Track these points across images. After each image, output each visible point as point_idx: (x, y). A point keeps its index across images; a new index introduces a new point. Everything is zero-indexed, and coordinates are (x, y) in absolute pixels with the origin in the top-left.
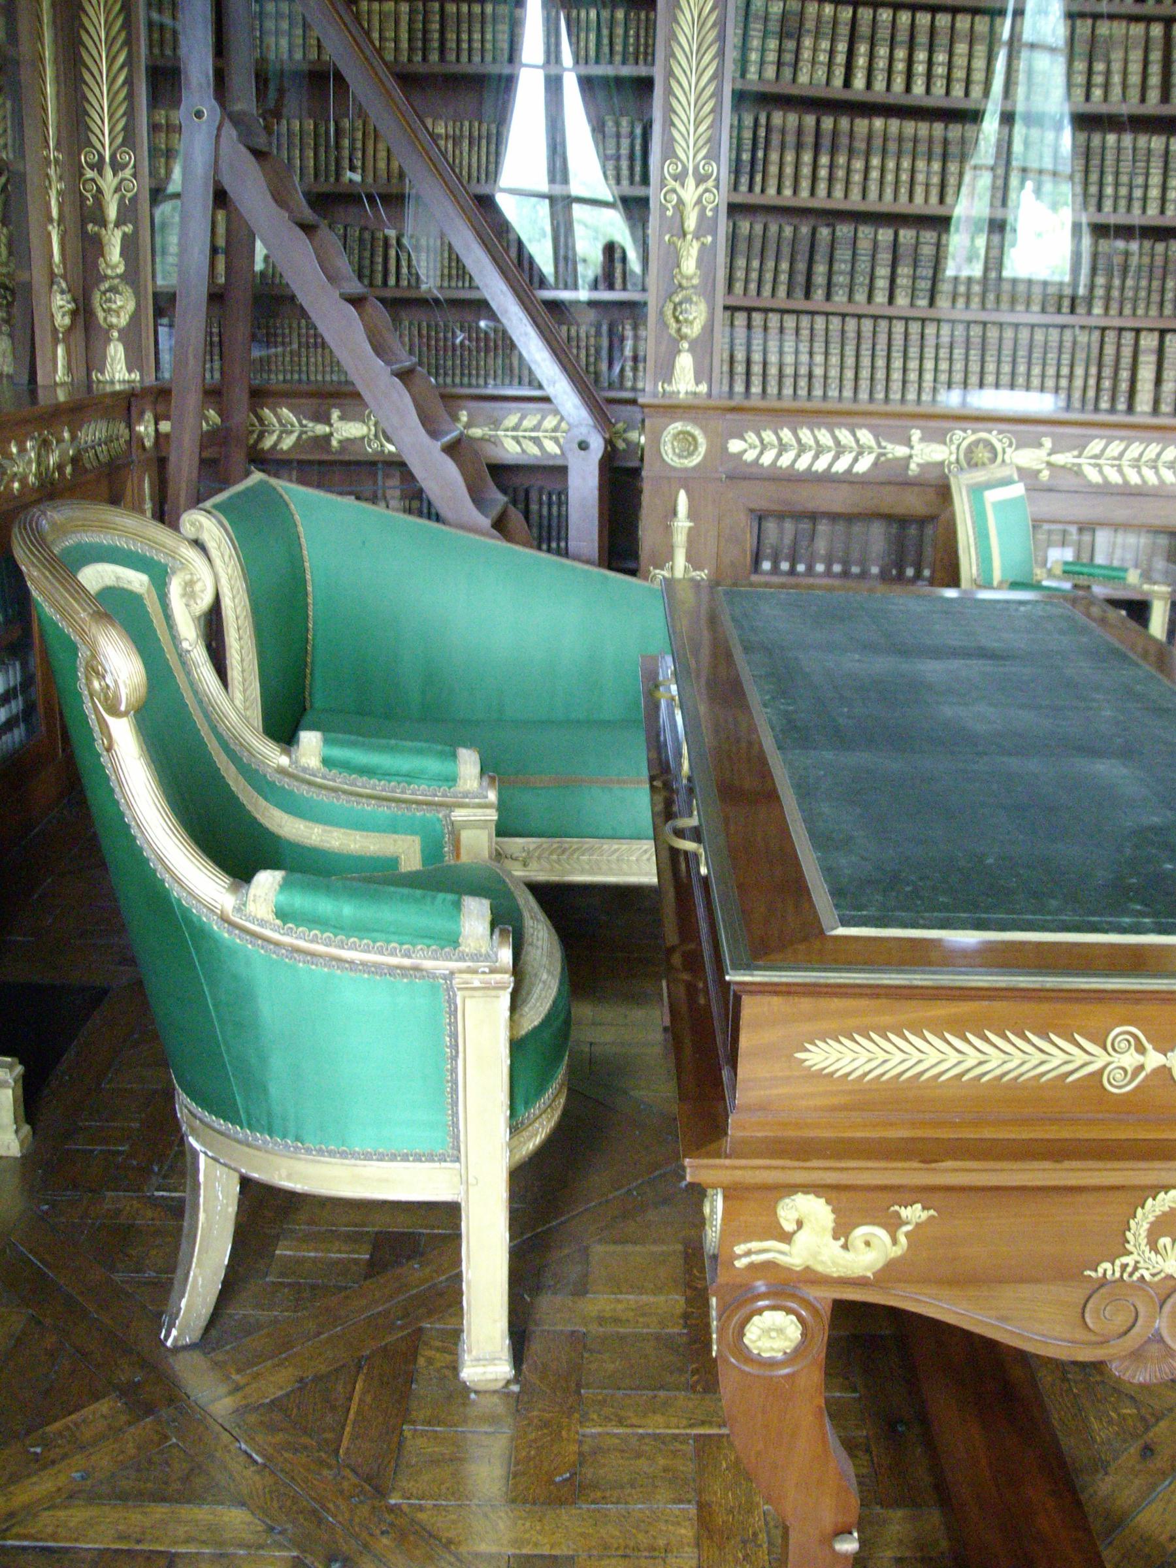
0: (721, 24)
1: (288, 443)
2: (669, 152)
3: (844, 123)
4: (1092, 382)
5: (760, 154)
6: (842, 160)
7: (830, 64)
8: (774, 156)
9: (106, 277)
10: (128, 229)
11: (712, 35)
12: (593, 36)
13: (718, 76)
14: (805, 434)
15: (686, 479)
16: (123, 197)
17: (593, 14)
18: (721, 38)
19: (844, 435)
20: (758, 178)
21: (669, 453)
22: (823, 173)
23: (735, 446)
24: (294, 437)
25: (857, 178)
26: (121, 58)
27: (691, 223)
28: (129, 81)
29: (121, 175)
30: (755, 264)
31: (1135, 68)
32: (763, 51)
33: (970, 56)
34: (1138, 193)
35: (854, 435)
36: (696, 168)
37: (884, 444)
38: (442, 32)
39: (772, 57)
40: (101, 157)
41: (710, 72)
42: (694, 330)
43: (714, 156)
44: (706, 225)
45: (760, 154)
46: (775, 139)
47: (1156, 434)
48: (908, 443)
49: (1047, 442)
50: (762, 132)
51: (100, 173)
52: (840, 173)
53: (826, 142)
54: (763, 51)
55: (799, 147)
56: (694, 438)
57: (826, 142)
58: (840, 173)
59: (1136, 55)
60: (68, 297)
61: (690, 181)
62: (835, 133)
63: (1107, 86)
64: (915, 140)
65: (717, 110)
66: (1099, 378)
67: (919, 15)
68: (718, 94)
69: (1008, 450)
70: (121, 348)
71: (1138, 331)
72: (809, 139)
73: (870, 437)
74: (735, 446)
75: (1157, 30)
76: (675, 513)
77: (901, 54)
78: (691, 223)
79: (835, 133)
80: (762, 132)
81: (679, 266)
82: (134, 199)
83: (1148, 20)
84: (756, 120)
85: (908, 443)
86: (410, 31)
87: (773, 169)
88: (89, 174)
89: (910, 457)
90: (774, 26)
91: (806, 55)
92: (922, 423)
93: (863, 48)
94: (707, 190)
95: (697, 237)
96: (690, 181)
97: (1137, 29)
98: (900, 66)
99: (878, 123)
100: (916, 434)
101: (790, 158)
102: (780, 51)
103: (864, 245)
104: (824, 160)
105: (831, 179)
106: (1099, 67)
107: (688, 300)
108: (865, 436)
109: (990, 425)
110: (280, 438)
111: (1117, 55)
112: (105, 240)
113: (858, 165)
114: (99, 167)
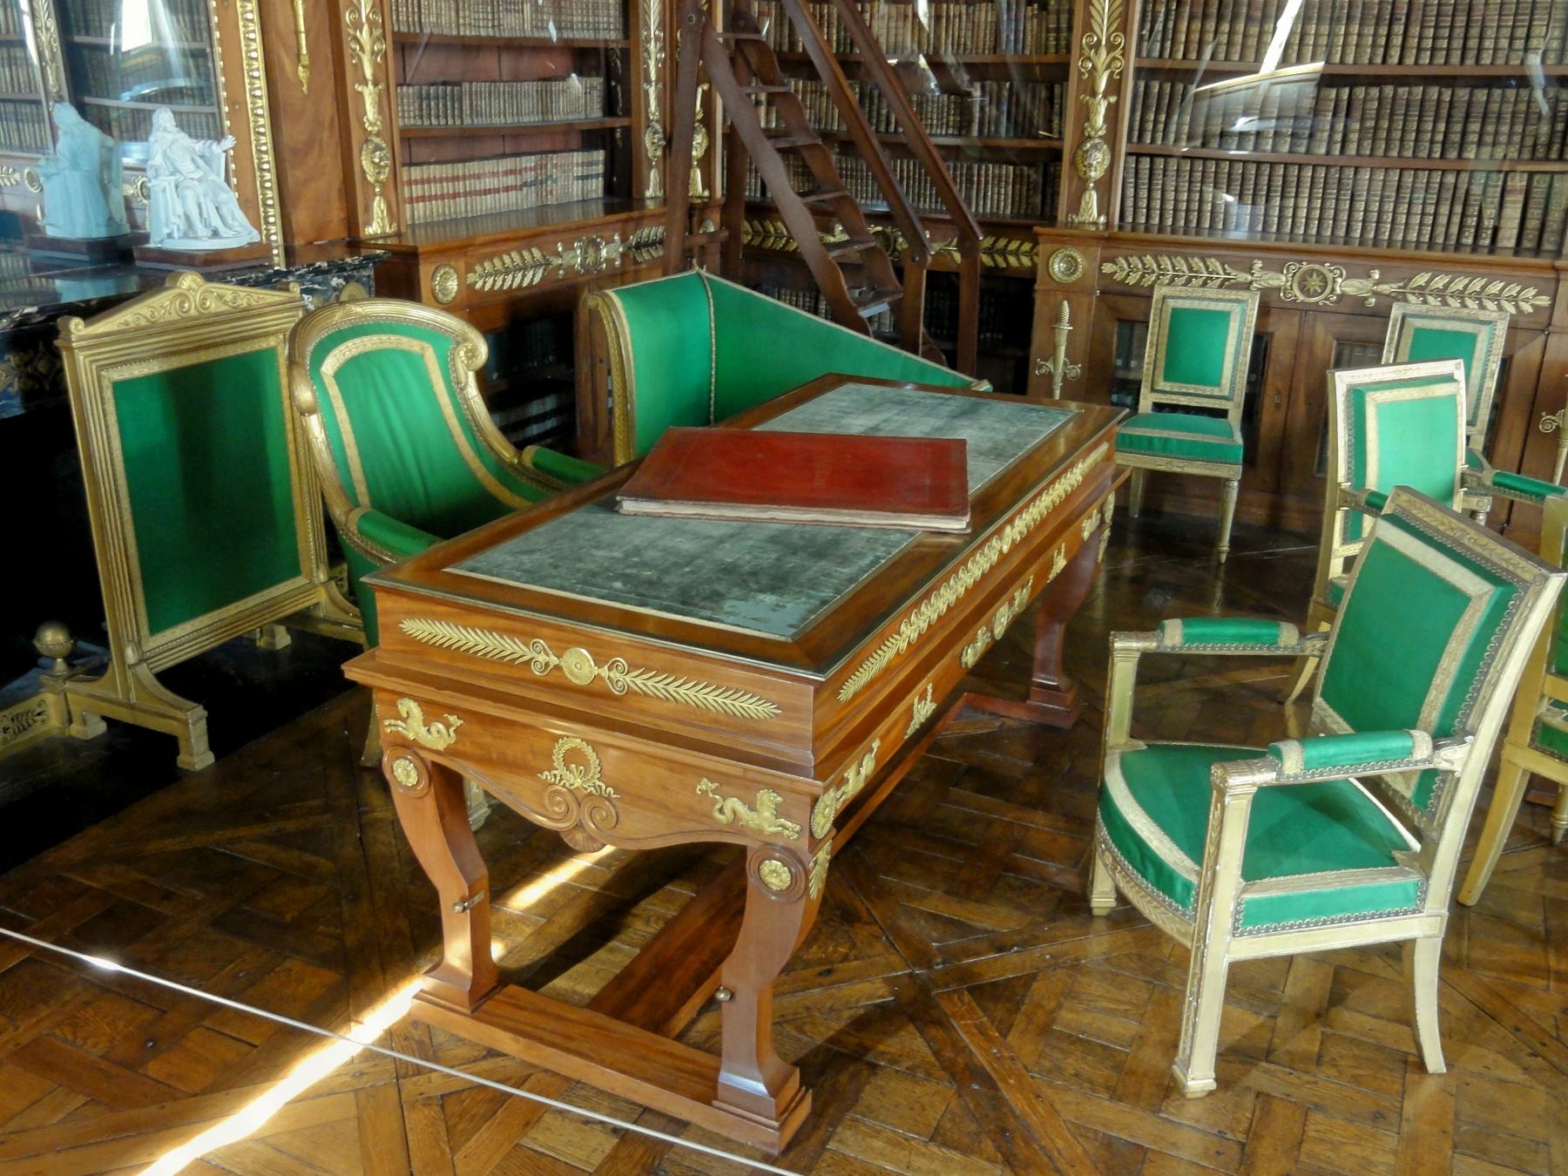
2: (1088, 28)
4: (1456, 219)
5: (1171, 25)
6: (1240, 27)
8: (1184, 26)
15: (1068, 291)
19: (1197, 263)
20: (1168, 44)
21: (1058, 267)
23: (1108, 268)
27: (1102, 85)
30: (1163, 117)
35: (1205, 264)
36: (1108, 39)
37: (1229, 270)
42: (1095, 174)
43: (1124, 28)
45: (1171, 25)
48: (1249, 270)
52: (1239, 39)
56: (1073, 258)
58: (1239, 39)
60: (661, 136)
61: (1103, 52)
66: (1464, 215)
69: (1339, 280)
73: (1218, 264)
74: (1108, 268)
78: (1102, 85)
81: (1088, 119)
85: (1249, 270)
89: (1251, 283)
94: (1115, 58)
95: (1105, 96)
96: (1103, 52)
100: (1259, 264)
101: (1197, 25)
107: (1095, 147)
108: (1214, 264)
109: (1320, 258)
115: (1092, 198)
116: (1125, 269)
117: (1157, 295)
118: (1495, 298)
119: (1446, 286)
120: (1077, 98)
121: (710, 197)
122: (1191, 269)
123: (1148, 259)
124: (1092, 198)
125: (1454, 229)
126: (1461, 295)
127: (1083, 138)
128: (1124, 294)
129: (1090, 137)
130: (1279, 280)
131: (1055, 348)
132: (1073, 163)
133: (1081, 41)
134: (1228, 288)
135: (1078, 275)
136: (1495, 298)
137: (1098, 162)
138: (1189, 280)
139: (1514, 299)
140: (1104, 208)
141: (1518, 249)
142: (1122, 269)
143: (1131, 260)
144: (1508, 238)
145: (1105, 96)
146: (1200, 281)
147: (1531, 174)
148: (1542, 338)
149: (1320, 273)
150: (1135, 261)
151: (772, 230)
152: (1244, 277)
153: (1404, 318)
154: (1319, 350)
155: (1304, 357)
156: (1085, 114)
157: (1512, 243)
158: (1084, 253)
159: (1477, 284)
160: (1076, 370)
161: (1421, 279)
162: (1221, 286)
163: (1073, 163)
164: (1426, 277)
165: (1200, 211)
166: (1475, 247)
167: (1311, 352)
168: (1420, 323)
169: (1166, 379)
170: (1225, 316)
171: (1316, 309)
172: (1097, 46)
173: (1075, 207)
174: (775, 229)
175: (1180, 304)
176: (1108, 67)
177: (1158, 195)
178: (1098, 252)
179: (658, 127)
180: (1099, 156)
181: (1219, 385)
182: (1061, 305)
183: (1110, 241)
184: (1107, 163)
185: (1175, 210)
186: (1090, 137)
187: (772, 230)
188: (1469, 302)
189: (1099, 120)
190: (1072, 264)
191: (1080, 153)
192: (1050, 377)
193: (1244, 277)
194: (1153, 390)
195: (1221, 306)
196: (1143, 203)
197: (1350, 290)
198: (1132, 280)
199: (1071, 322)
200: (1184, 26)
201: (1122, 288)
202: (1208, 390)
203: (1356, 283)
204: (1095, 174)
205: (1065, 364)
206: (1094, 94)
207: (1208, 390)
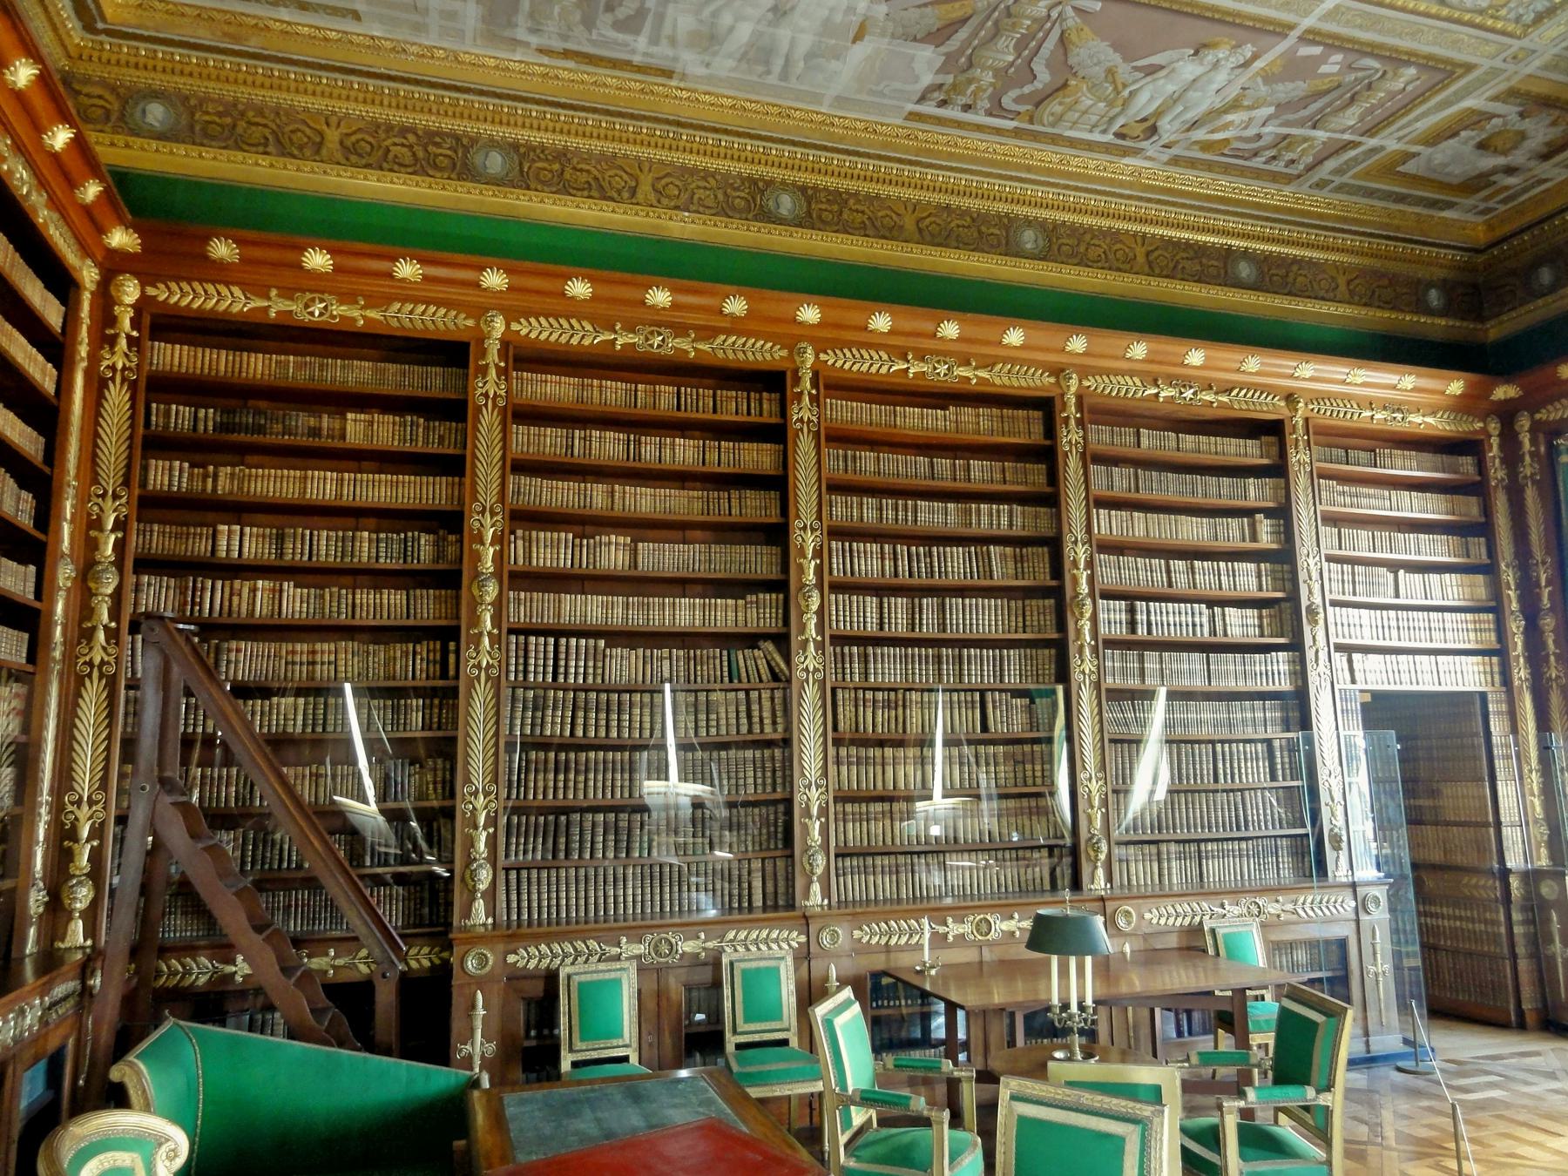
0: (498, 705)
1: (203, 980)
2: (468, 781)
3: (572, 756)
5: (523, 776)
6: (572, 776)
7: (562, 723)
9: (74, 876)
10: (95, 844)
11: (493, 712)
12: (420, 714)
13: (497, 734)
14: (556, 947)
15: (480, 983)
16: (94, 823)
17: (421, 702)
18: (497, 713)
19: (580, 945)
21: (471, 964)
22: (561, 784)
23: (511, 959)
24: (207, 977)
25: (581, 786)
26: (104, 735)
27: (482, 820)
28: (108, 749)
29: (94, 808)
31: (733, 715)
32: (523, 718)
33: (641, 715)
34: (741, 782)
36: (484, 788)
38: (325, 714)
40: (81, 798)
41: (491, 733)
42: (482, 887)
44: (492, 821)
45: (523, 776)
46: (533, 766)
47: (766, 923)
48: (619, 945)
49: (702, 936)
51: (79, 807)
52: (571, 784)
53: (562, 767)
55: (546, 771)
56: (485, 956)
57: (562, 767)
58: (571, 784)
59: (732, 708)
60: (44, 892)
62: (567, 761)
63: (718, 726)
64: (613, 762)
65: (496, 754)
67: (611, 695)
68: (497, 744)
70: (80, 923)
71: (749, 860)
72: (552, 766)
74: (511, 959)
75: (742, 695)
76: (473, 1006)
77: (603, 715)
78: (482, 820)
79: (567, 761)
81: (473, 846)
82: (102, 824)
83: (736, 690)
85: (619, 945)
86: (304, 714)
88: (70, 808)
91: (549, 719)
92: (625, 932)
93: (581, 714)
95: (485, 828)
97: (731, 695)
98: (603, 723)
99: (592, 755)
100: (624, 940)
101: (541, 776)
103: (588, 825)
104: (561, 777)
105: (566, 787)
106: (713, 716)
107: (480, 866)
108: (593, 944)
110: (197, 978)
111: (722, 710)
112: (76, 852)
113: (581, 778)
114: (79, 803)
115: (480, 905)
116: (529, 958)
117: (562, 975)
118: (776, 941)
119: (746, 938)
120: (463, 831)
121: (93, 947)
122: (575, 949)
123: (543, 947)
124: (480, 905)
125: (727, 899)
126: (756, 942)
127: (470, 860)
128: (525, 978)
129: (475, 859)
130: (639, 949)
131: (472, 1030)
132: (463, 880)
133: (463, 790)
134: (605, 961)
135: (488, 968)
136: (776, 941)
137: (484, 877)
138: (576, 959)
139: (787, 940)
140: (491, 911)
141: (765, 908)
142: (523, 958)
143: (589, 942)
144: (758, 901)
145: (485, 828)
146: (584, 958)
147: (763, 860)
148: (806, 963)
149: (667, 940)
150: (532, 950)
151: (165, 969)
152: (615, 951)
153: (732, 964)
154: (674, 996)
155: (664, 1003)
156: (471, 843)
157: (760, 904)
158: (492, 950)
159: (764, 933)
160: (491, 1048)
161: (731, 935)
162: (599, 960)
163: (463, 880)
164: (734, 933)
165: (558, 905)
166: (740, 908)
167: (668, 999)
168: (743, 965)
169: (582, 1040)
170: (618, 982)
171: (668, 967)
172: (475, 794)
173: (467, 913)
174: (169, 967)
175: (583, 978)
176: (486, 807)
177: (525, 897)
178: (501, 947)
179: (41, 885)
180: (484, 872)
181: (622, 1036)
182: (475, 995)
183: (511, 934)
184: (490, 877)
185: (539, 907)
186: (475, 859)
187: (165, 969)
188: (761, 946)
189: (481, 845)
190: (483, 960)
191: (468, 872)
192: (470, 1057)
193: (615, 951)
194: (571, 1050)
195: (613, 975)
196: (514, 905)
197: (687, 949)
198: (531, 965)
199: (484, 1007)
200: (532, 777)
201: (524, 973)
202: (615, 1042)
203: (691, 943)
204: (482, 887)
205: (482, 1044)
206: (476, 827)
207: (615, 1042)
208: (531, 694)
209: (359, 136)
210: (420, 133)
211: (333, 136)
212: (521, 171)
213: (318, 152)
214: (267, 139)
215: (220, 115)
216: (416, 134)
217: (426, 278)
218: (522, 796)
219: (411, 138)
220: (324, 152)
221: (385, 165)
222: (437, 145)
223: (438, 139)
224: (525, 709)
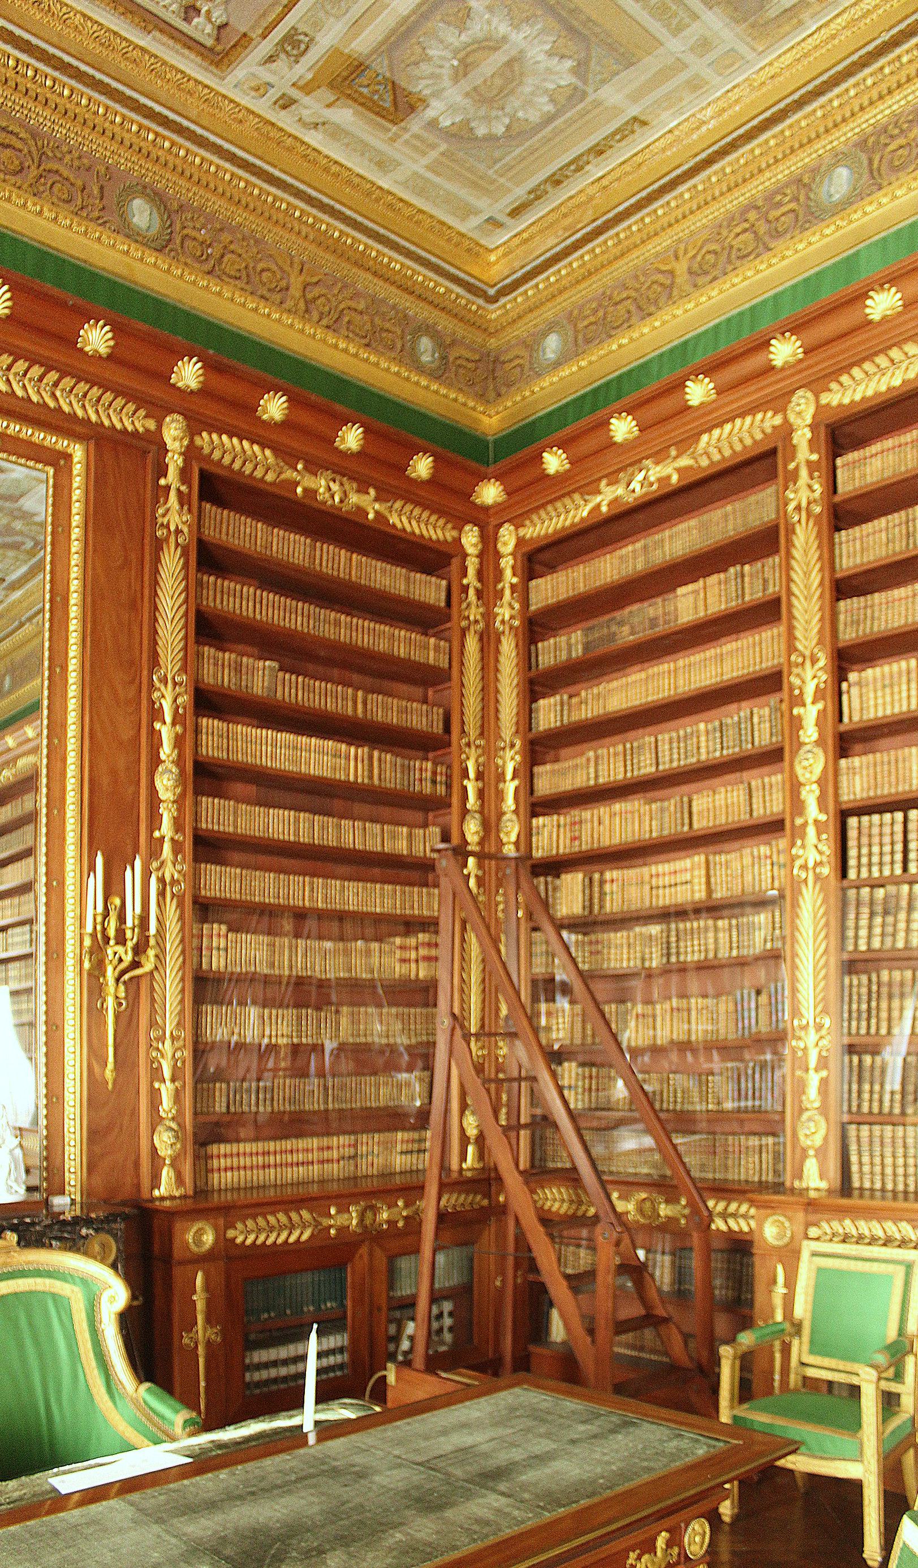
8: (884, 1005)
20: (873, 1021)
32: (870, 927)
39: (878, 930)
44: (823, 1063)
45: (874, 1004)
46: (884, 990)
50: (874, 988)
54: (870, 927)
80: (874, 988)
81: (804, 1093)
84: (870, 980)
87: (884, 1015)
90: (879, 909)
102: (883, 925)
172: (805, 1028)
173: (799, 1175)
208: (880, 893)
209: (704, 251)
210: (760, 203)
211: (681, 268)
212: (871, 171)
213: (670, 297)
214: (629, 312)
215: (595, 311)
216: (757, 208)
217: (720, 391)
218: (873, 1030)
219: (752, 216)
220: (675, 292)
221: (730, 268)
222: (780, 204)
223: (779, 198)
224: (872, 914)
